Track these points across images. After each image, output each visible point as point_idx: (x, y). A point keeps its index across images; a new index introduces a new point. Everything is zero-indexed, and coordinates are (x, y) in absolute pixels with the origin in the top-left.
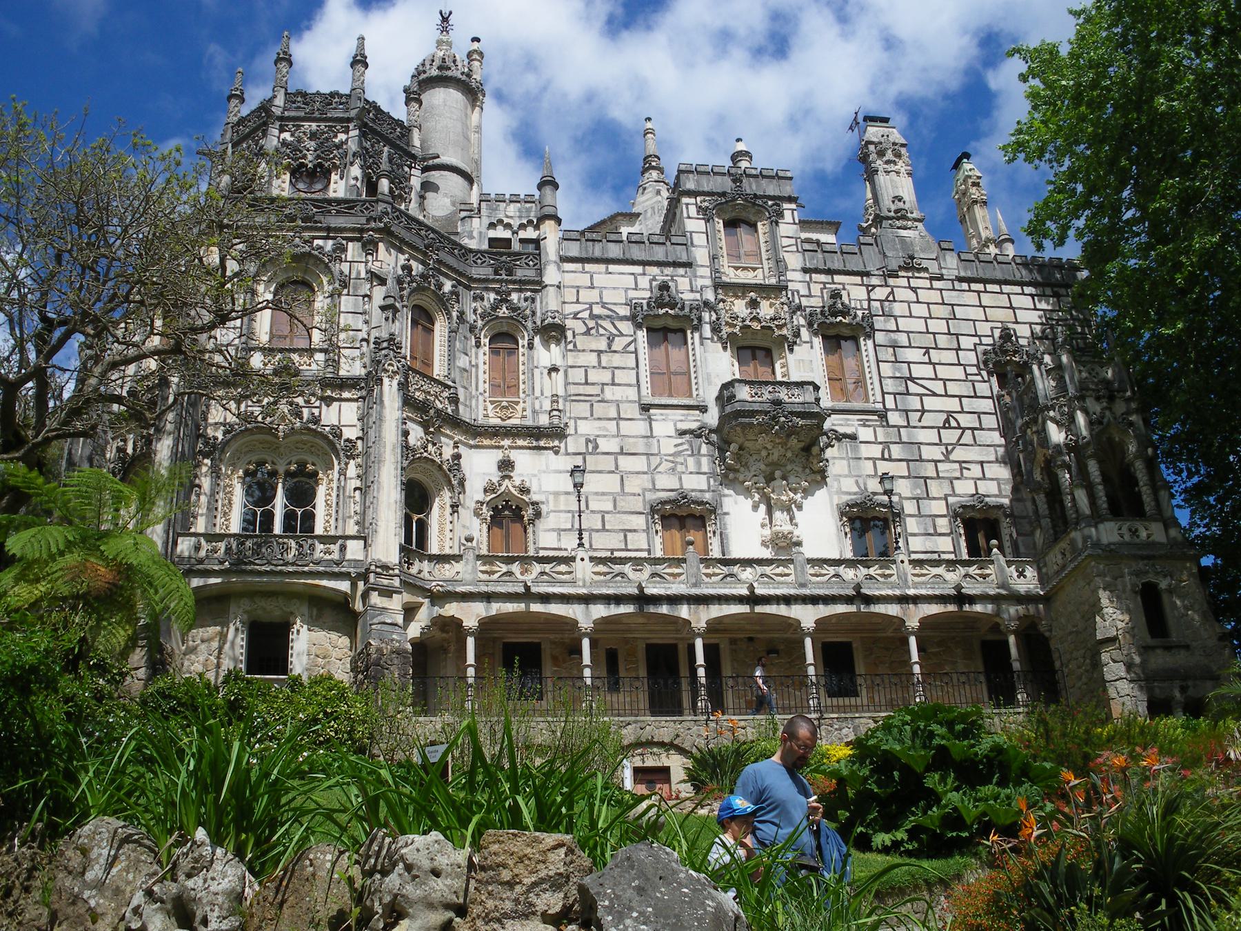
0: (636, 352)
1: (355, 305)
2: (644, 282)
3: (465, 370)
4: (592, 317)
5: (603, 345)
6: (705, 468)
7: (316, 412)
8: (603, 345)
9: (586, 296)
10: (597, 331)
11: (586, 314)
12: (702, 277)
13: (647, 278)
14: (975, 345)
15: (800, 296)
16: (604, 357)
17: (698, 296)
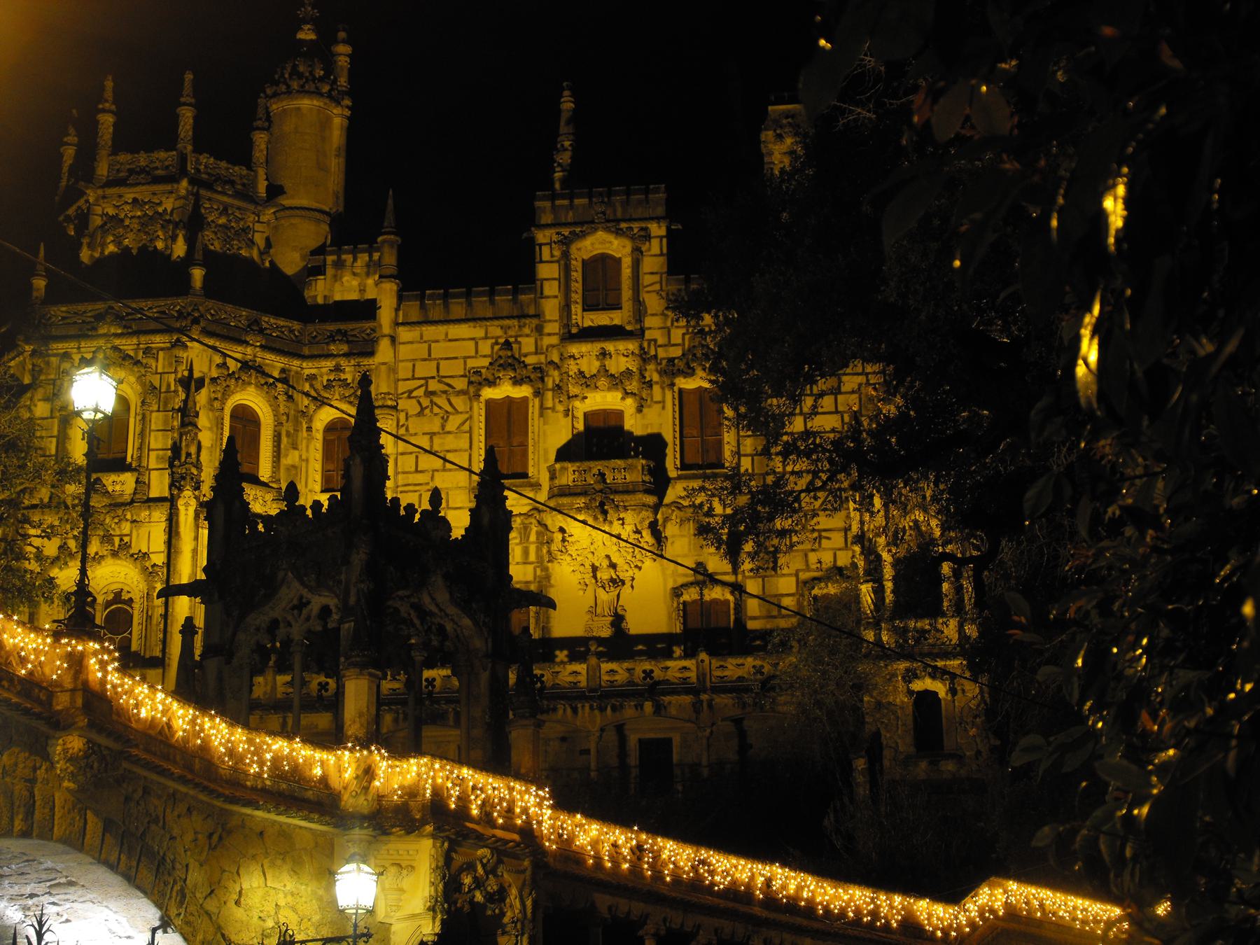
0: (470, 431)
1: (166, 422)
2: (485, 348)
3: (294, 467)
4: (429, 394)
5: (436, 428)
6: (532, 557)
7: (126, 539)
8: (436, 427)
9: (425, 370)
10: (431, 411)
11: (421, 392)
12: (549, 334)
13: (490, 342)
14: (860, 385)
15: (657, 346)
16: (437, 440)
17: (542, 358)
